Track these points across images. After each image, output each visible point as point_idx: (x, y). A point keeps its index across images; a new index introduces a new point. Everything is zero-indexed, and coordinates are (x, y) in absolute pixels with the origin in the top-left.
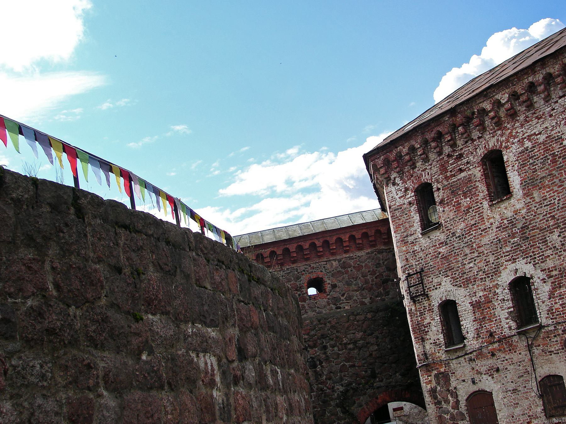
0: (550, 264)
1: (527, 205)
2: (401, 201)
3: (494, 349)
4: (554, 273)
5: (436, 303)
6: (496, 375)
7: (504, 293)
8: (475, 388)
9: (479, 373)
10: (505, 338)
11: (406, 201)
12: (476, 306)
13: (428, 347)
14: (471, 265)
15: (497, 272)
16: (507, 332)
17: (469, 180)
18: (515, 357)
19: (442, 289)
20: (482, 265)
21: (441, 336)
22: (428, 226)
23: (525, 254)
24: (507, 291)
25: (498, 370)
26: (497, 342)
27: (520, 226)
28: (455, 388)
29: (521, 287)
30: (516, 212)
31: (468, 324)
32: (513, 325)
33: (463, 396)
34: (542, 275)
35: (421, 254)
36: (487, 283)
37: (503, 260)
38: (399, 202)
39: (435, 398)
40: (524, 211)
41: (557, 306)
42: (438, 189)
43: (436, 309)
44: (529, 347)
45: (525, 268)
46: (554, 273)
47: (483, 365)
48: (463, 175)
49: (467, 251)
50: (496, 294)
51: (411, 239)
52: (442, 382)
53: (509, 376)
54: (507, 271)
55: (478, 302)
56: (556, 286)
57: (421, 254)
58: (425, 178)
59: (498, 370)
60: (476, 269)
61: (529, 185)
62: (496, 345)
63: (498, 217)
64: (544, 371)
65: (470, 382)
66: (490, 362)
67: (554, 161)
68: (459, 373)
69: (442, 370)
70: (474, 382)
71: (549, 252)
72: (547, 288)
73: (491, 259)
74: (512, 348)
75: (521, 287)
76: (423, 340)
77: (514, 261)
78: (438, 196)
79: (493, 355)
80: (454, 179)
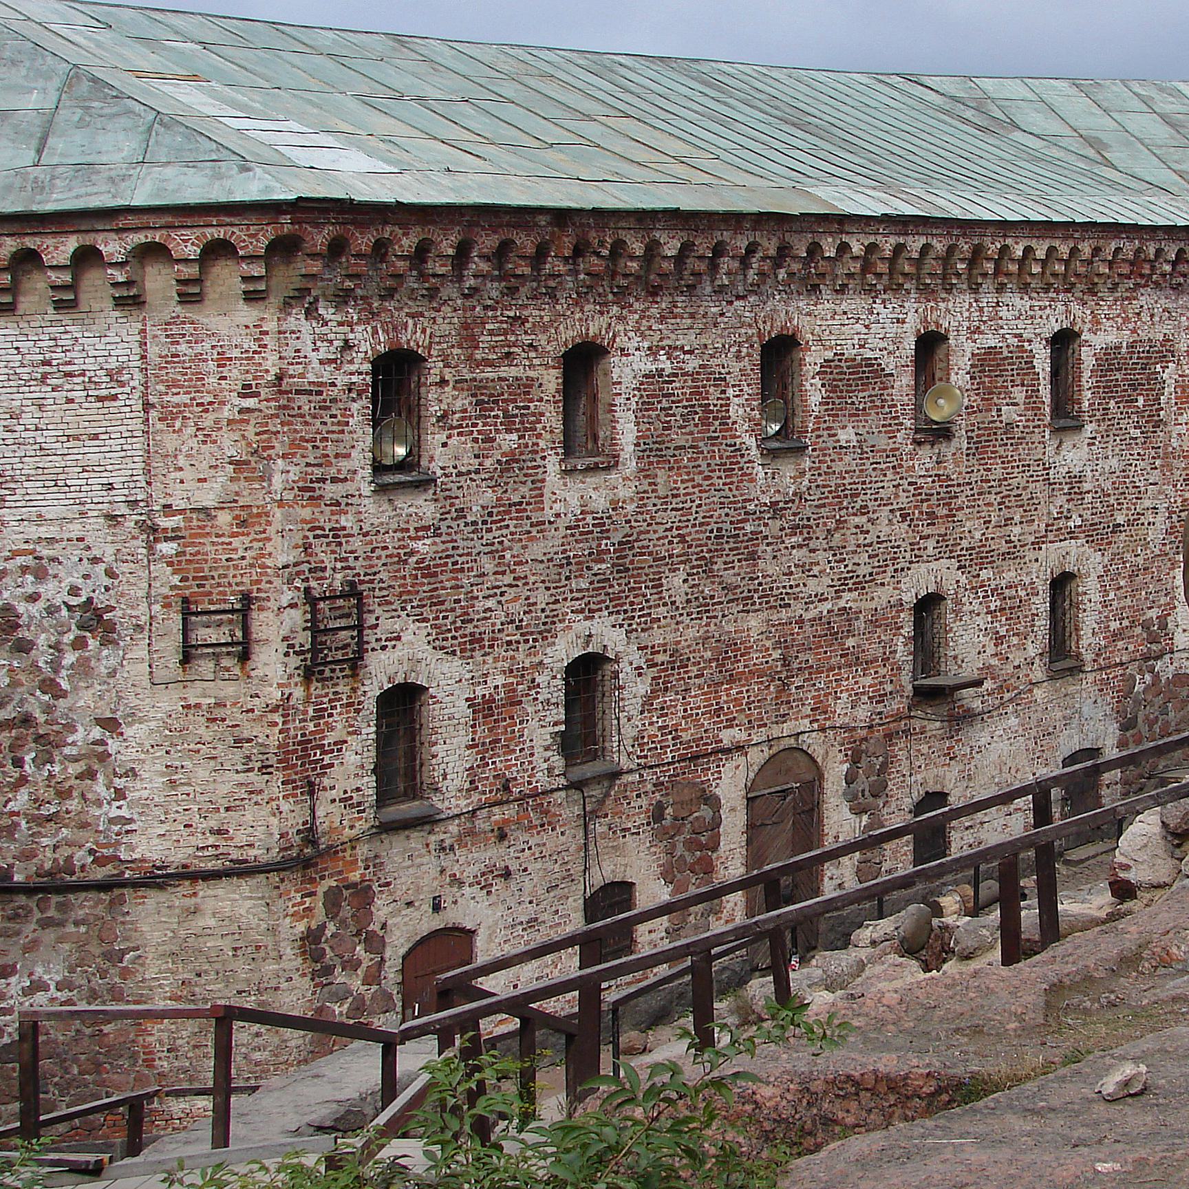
0: (657, 637)
1: (641, 496)
2: (327, 374)
3: (506, 821)
4: (660, 658)
5: (373, 689)
6: (498, 885)
7: (552, 687)
8: (437, 923)
9: (457, 881)
10: (535, 794)
11: (341, 380)
12: (483, 709)
13: (320, 812)
14: (491, 603)
15: (546, 633)
16: (542, 780)
17: (526, 387)
18: (551, 840)
19: (401, 652)
20: (517, 608)
21: (369, 783)
22: (396, 476)
23: (616, 604)
24: (559, 682)
25: (507, 874)
26: (509, 804)
27: (617, 537)
28: (384, 926)
29: (587, 674)
30: (615, 505)
31: (450, 754)
32: (558, 761)
33: (397, 946)
34: (638, 659)
35: (356, 543)
36: (520, 656)
37: (566, 607)
38: (316, 373)
39: (318, 956)
40: (631, 508)
41: (652, 730)
42: (443, 382)
43: (370, 705)
44: (587, 819)
45: (607, 634)
46: (660, 658)
47: (470, 862)
48: (513, 372)
49: (489, 565)
50: (533, 685)
51: (331, 491)
52: (346, 911)
53: (528, 886)
54: (571, 635)
55: (489, 702)
56: (660, 687)
57: (356, 543)
58: (413, 337)
59: (507, 874)
60: (499, 617)
61: (653, 451)
62: (510, 811)
63: (574, 502)
64: (606, 871)
65: (427, 908)
66: (494, 854)
67: (705, 422)
68: (403, 884)
69: (355, 876)
70: (437, 907)
71: (662, 610)
72: (642, 687)
73: (542, 598)
74: (548, 822)
75: (587, 674)
76: (311, 789)
77: (590, 614)
78: (435, 401)
79: (502, 837)
80: (489, 373)
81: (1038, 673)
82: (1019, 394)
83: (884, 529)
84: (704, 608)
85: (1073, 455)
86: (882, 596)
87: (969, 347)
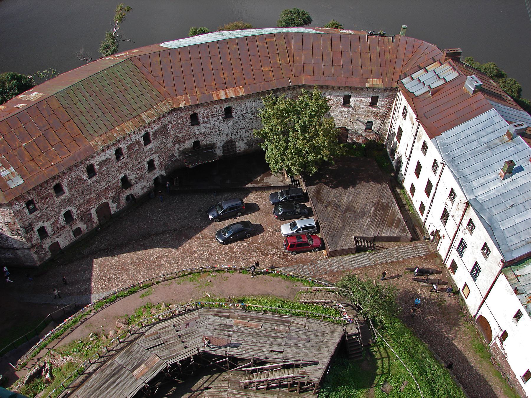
81: (147, 173)
82: (137, 146)
83: (113, 174)
84: (83, 198)
85: (149, 146)
86: (114, 181)
87: (125, 147)
